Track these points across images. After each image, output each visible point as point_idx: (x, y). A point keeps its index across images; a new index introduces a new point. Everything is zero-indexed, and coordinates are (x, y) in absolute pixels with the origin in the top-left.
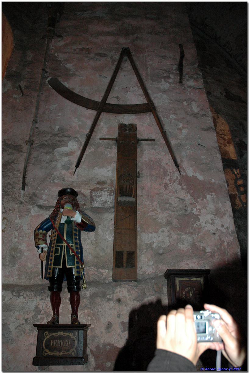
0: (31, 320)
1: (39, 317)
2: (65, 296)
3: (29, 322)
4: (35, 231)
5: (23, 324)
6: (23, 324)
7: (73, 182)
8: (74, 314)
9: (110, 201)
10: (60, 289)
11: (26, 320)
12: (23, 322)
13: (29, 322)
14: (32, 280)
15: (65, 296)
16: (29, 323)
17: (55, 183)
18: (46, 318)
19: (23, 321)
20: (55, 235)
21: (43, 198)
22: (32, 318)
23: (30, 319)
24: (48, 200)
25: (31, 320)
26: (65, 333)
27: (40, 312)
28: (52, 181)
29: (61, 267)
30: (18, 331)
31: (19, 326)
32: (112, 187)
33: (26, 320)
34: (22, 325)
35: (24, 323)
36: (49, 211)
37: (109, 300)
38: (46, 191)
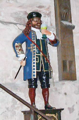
0: (11, 108)
1: (16, 106)
2: (39, 91)
3: (9, 110)
4: (14, 44)
5: (6, 111)
6: (6, 111)
7: (23, 4)
8: (46, 102)
9: (45, 21)
10: (36, 86)
11: (7, 109)
12: (6, 110)
13: (9, 110)
14: (4, 80)
15: (39, 91)
16: (10, 111)
17: (10, 3)
18: (21, 107)
19: (6, 109)
20: (35, 48)
21: (2, 15)
22: (11, 107)
23: (10, 108)
24: (5, 17)
25: (11, 108)
26: (50, 115)
27: (17, 103)
28: (8, 1)
29: (40, 71)
30: (3, 116)
31: (3, 113)
32: (47, 11)
33: (7, 109)
34: (5, 112)
35: (6, 110)
36: (9, 26)
37: (59, 93)
38: (3, 9)
